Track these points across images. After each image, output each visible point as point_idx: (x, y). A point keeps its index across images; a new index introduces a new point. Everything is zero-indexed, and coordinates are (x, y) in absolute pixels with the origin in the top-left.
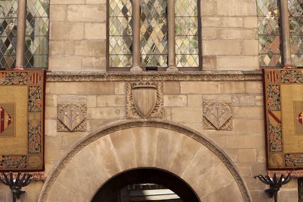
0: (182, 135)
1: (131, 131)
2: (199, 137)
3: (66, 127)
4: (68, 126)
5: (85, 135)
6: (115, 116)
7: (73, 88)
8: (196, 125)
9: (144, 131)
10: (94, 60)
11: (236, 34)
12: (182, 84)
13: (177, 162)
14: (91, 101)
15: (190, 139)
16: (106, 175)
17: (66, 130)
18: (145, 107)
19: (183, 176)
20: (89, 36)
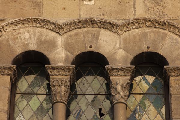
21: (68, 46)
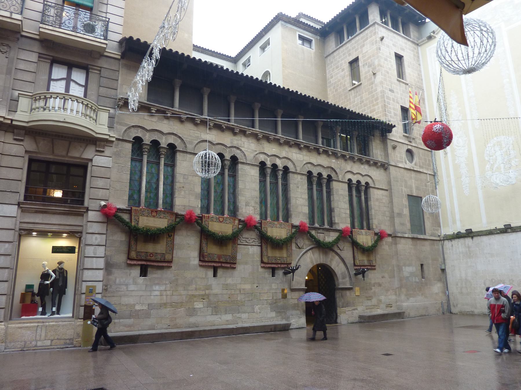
5: (305, 250)
11: (344, 215)
12: (331, 233)
17: (298, 247)
20: (304, 211)
21: (270, 161)
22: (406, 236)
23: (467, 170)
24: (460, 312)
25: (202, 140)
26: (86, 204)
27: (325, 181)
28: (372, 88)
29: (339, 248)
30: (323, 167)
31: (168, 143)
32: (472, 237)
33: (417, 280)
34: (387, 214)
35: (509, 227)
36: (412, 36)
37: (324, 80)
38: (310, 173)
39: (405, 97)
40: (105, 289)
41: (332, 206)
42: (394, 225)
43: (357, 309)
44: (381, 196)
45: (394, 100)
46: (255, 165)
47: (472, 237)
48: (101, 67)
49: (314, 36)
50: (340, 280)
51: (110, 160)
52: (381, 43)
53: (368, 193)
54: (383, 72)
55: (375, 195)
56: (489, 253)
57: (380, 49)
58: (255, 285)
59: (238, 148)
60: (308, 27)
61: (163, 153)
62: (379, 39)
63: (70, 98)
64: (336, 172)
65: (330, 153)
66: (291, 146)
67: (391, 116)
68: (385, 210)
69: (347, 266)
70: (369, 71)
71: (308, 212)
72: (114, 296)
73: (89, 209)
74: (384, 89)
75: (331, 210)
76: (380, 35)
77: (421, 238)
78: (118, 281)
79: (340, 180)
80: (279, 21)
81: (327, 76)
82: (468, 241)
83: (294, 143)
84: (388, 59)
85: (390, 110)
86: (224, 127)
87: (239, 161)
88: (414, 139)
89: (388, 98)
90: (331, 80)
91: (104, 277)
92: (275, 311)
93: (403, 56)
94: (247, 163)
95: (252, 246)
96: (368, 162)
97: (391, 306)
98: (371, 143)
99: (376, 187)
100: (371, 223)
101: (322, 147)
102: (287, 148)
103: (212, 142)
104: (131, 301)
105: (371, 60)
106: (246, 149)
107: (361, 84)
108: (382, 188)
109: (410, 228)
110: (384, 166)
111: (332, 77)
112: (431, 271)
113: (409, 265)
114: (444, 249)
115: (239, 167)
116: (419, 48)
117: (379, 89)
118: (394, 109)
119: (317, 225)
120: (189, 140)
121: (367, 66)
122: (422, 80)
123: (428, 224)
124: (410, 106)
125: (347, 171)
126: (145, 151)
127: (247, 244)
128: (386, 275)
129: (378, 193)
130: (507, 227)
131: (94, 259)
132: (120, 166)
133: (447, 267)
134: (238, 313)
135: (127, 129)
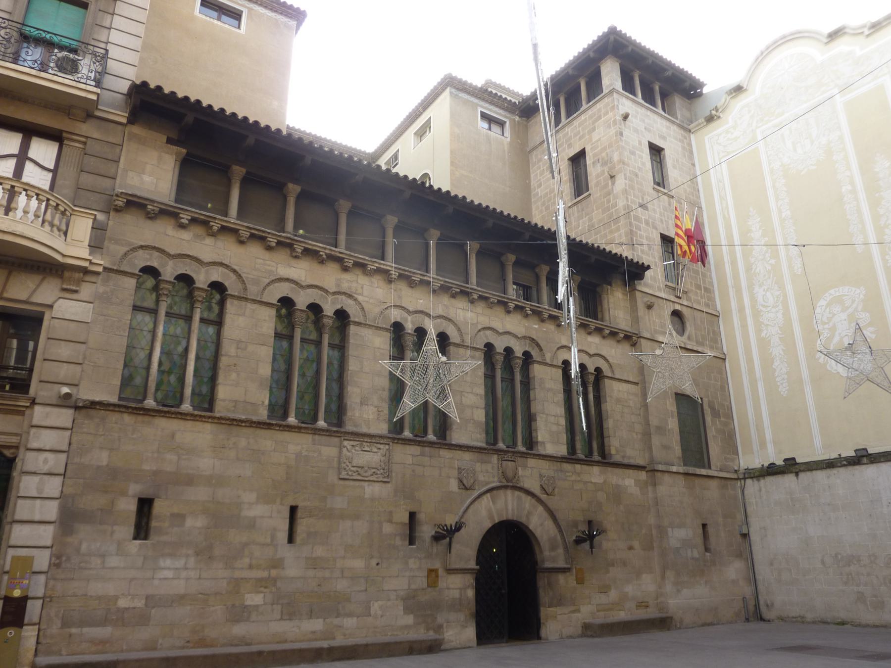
0: (529, 497)
1: (501, 492)
2: (539, 500)
3: (464, 485)
4: (466, 485)
5: (476, 493)
6: (491, 479)
7: (467, 456)
8: (537, 491)
9: (509, 492)
10: (479, 436)
12: (529, 460)
13: (528, 517)
14: (478, 467)
15: (533, 501)
16: (488, 525)
17: (463, 487)
18: (510, 474)
19: (531, 527)
20: (476, 418)
21: (413, 322)
22: (674, 469)
23: (783, 350)
24: (778, 618)
25: (279, 277)
26: (32, 391)
27: (520, 362)
28: (609, 201)
29: (545, 491)
30: (516, 336)
31: (209, 282)
32: (797, 474)
33: (696, 554)
34: (638, 428)
35: (864, 453)
36: (679, 116)
37: (526, 189)
38: (489, 347)
39: (668, 218)
40: (57, 562)
41: (533, 410)
42: (650, 449)
43: (578, 611)
44: (625, 394)
45: (647, 223)
46: (383, 328)
47: (797, 474)
48: (87, 137)
49: (509, 115)
50: (547, 553)
51: (90, 309)
52: (625, 124)
53: (601, 387)
54: (628, 174)
55: (614, 391)
56: (829, 504)
57: (621, 134)
58: (374, 562)
59: (350, 296)
60: (499, 100)
61: (200, 299)
62: (619, 118)
63: (25, 190)
64: (540, 346)
65: (529, 312)
66: (453, 296)
67: (642, 251)
68: (633, 420)
69: (560, 526)
70: (603, 172)
71: (484, 420)
72: (73, 579)
73: (37, 401)
74: (629, 203)
75: (530, 419)
76: (623, 110)
77: (702, 474)
78: (84, 548)
79: (548, 361)
80: (446, 88)
81: (532, 184)
82: (788, 480)
83: (459, 290)
84: (637, 152)
85: (641, 240)
86: (324, 256)
87: (352, 319)
88: (685, 292)
89: (637, 218)
90: (539, 190)
91: (54, 538)
92: (412, 613)
93: (663, 149)
94: (365, 324)
95: (371, 483)
96: (599, 330)
97: (646, 604)
98: (605, 296)
99: (617, 376)
100: (606, 444)
101: (515, 300)
102: (445, 299)
103: (299, 282)
104: (110, 589)
105: (607, 154)
106: (367, 299)
107: (590, 194)
108: (627, 379)
109: (680, 455)
110: (631, 339)
111: (540, 186)
112: (720, 537)
113: (681, 526)
114: (746, 497)
115: (351, 332)
116: (692, 136)
117: (621, 203)
118: (648, 238)
119: (501, 445)
120: (252, 277)
121: (599, 165)
122: (699, 191)
123: (715, 449)
124: (677, 234)
125: (560, 345)
126: (164, 294)
127: (360, 478)
128: (636, 544)
129: (621, 389)
130: (860, 454)
131: (38, 502)
132: (107, 320)
133: (752, 530)
134: (336, 617)
135: (128, 251)
